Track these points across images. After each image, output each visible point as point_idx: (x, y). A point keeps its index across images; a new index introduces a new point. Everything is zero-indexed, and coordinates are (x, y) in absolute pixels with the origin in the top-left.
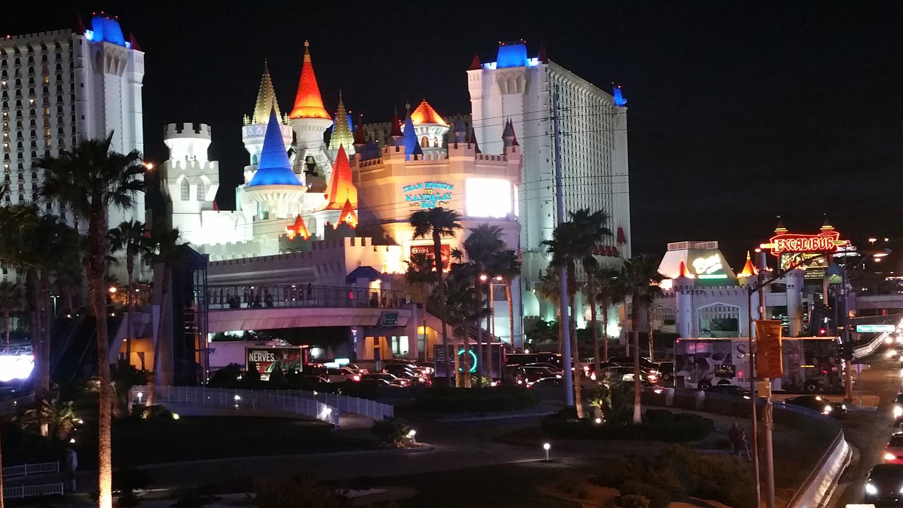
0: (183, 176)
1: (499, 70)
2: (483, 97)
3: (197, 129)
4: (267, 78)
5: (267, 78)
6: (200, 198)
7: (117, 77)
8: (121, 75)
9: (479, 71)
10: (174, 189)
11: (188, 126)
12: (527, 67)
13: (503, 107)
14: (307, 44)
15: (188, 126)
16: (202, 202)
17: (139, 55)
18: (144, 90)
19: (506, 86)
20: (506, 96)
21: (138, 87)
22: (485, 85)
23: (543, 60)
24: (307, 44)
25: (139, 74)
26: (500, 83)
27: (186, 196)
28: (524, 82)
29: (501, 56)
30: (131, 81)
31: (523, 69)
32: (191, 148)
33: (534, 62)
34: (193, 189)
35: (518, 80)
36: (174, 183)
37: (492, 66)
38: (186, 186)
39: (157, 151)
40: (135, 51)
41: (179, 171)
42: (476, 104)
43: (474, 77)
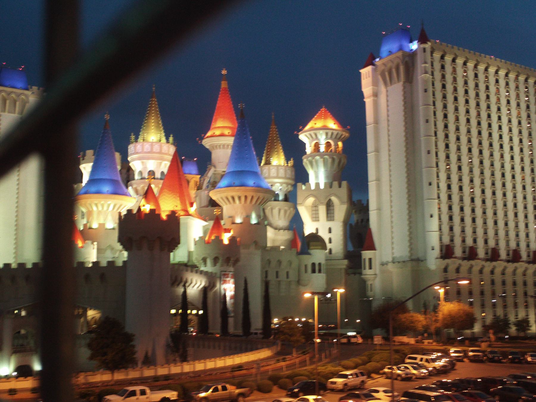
9: (369, 68)
20: (390, 88)
22: (375, 83)
28: (402, 68)
33: (414, 46)
37: (377, 60)
42: (369, 102)
43: (366, 72)
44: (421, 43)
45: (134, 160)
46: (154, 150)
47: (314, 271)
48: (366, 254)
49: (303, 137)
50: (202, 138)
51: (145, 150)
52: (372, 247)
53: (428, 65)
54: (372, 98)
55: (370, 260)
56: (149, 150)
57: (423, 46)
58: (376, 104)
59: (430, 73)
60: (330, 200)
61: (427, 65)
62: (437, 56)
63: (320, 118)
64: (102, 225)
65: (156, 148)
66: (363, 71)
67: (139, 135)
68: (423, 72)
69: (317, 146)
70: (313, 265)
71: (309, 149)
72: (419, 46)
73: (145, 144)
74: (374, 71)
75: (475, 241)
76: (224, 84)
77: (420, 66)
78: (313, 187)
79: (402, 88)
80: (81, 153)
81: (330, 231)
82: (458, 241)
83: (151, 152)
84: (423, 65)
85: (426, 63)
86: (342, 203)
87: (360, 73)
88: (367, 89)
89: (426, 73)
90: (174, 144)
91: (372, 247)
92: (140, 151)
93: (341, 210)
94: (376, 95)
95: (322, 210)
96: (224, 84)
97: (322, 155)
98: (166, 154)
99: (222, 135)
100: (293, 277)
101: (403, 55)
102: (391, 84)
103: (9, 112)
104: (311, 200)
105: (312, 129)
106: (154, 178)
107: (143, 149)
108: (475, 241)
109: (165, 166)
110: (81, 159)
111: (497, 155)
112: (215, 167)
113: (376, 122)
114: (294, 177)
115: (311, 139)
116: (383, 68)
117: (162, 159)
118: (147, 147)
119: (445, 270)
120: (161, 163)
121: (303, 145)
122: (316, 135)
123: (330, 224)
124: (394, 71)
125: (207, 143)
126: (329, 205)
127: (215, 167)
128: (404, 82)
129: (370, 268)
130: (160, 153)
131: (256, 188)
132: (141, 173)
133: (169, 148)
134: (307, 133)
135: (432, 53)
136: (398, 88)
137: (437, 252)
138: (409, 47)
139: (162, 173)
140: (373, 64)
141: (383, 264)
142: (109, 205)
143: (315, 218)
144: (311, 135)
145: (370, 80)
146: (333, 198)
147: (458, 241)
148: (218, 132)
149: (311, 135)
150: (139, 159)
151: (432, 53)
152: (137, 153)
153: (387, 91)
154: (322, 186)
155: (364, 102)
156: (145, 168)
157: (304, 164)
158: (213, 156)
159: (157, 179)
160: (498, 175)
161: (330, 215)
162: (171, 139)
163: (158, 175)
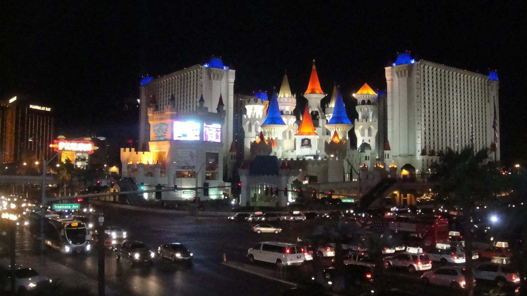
0: (248, 122)
2: (392, 80)
4: (286, 77)
5: (286, 77)
6: (256, 131)
7: (219, 81)
8: (221, 80)
10: (246, 127)
14: (314, 61)
15: (252, 100)
17: (232, 72)
18: (234, 86)
19: (399, 74)
20: (401, 79)
21: (232, 86)
22: (392, 75)
23: (417, 60)
25: (232, 79)
26: (397, 73)
27: (250, 130)
28: (407, 72)
29: (399, 60)
30: (228, 82)
32: (253, 109)
33: (413, 62)
34: (253, 127)
35: (405, 71)
36: (245, 124)
37: (394, 65)
38: (250, 125)
39: (240, 110)
40: (230, 70)
41: (247, 119)
42: (389, 83)
47: (366, 159)
48: (386, 152)
50: (304, 94)
52: (389, 149)
55: (388, 155)
58: (392, 85)
62: (422, 66)
63: (365, 88)
64: (277, 138)
66: (387, 69)
70: (366, 157)
74: (391, 69)
75: (434, 148)
76: (314, 67)
77: (415, 71)
81: (369, 141)
82: (428, 147)
83: (288, 102)
88: (388, 76)
89: (418, 75)
90: (297, 98)
91: (389, 149)
93: (375, 132)
94: (392, 80)
95: (366, 131)
96: (314, 67)
100: (358, 162)
104: (361, 127)
105: (362, 94)
108: (434, 148)
111: (444, 109)
113: (392, 92)
119: (423, 161)
123: (370, 138)
126: (369, 129)
129: (388, 158)
130: (292, 103)
136: (404, 80)
137: (420, 153)
140: (392, 66)
141: (393, 156)
143: (363, 135)
145: (390, 72)
146: (371, 127)
147: (428, 147)
157: (356, 109)
158: (309, 102)
161: (370, 134)
162: (295, 96)
163: (290, 113)
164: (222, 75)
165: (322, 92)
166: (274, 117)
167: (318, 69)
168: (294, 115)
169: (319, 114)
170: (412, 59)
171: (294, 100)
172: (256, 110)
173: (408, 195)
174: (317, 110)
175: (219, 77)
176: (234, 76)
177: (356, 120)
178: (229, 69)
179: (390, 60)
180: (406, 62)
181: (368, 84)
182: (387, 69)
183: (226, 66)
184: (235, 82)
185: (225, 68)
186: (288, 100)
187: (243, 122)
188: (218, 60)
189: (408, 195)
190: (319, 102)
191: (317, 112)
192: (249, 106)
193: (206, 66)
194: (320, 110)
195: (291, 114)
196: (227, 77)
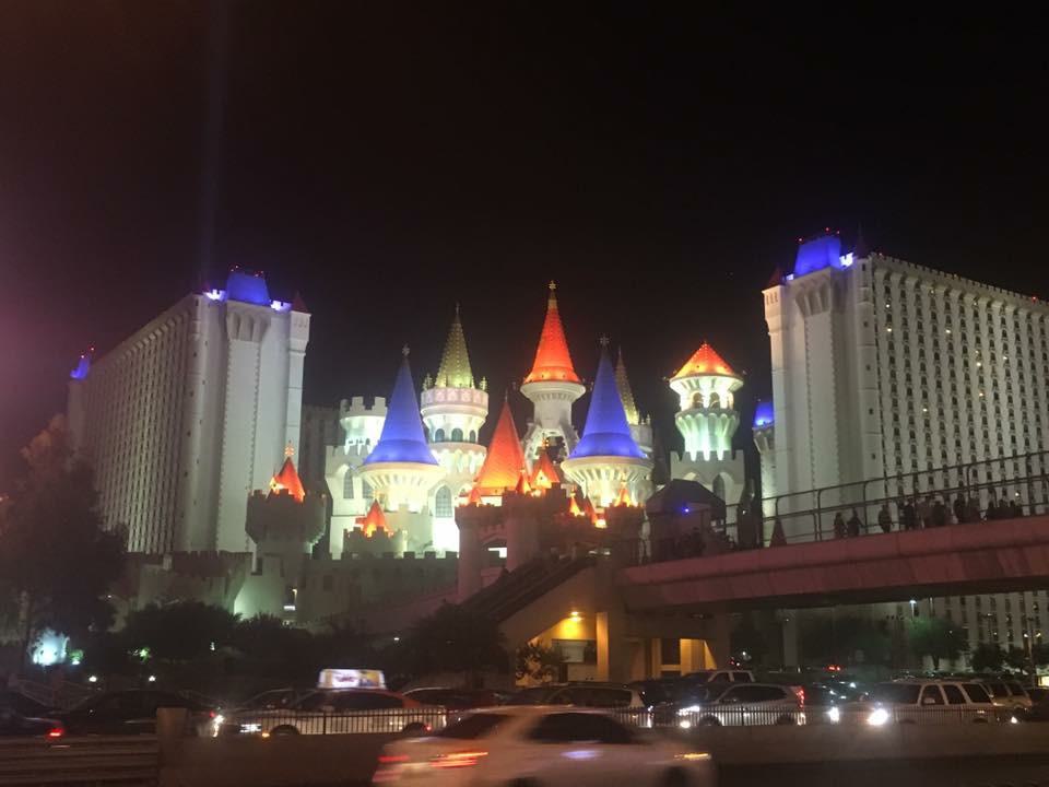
0: (344, 469)
1: (796, 280)
3: (369, 405)
7: (254, 344)
8: (261, 339)
10: (335, 486)
11: (358, 401)
12: (833, 269)
13: (806, 337)
15: (358, 401)
16: (370, 501)
20: (810, 319)
23: (859, 255)
24: (552, 286)
25: (300, 340)
27: (349, 494)
28: (830, 292)
31: (827, 272)
37: (791, 277)
44: (859, 258)
45: (431, 413)
46: (463, 399)
49: (676, 385)
50: (521, 383)
51: (449, 399)
53: (869, 289)
54: (780, 332)
56: (456, 398)
57: (862, 261)
59: (871, 299)
60: (719, 476)
61: (868, 289)
62: (880, 274)
63: (701, 358)
65: (466, 396)
67: (436, 376)
68: (863, 298)
69: (697, 397)
71: (685, 403)
72: (854, 261)
73: (449, 390)
76: (552, 304)
78: (693, 458)
79: (829, 319)
80: (344, 402)
84: (863, 289)
85: (866, 286)
86: (736, 481)
87: (763, 295)
88: (773, 319)
89: (866, 299)
90: (488, 390)
92: (442, 399)
94: (786, 327)
96: (552, 304)
97: (706, 413)
98: (478, 405)
99: (553, 380)
101: (833, 274)
102: (813, 313)
103: (244, 339)
106: (461, 441)
107: (446, 397)
109: (477, 423)
110: (343, 409)
112: (540, 424)
114: (651, 442)
115: (689, 387)
116: (800, 289)
117: (473, 413)
118: (452, 395)
120: (470, 420)
121: (675, 397)
122: (697, 382)
124: (818, 295)
125: (528, 389)
127: (540, 424)
128: (833, 312)
130: (471, 403)
131: (632, 459)
132: (440, 432)
133: (482, 396)
134: (684, 381)
135: (873, 270)
136: (824, 319)
138: (839, 262)
139: (472, 433)
142: (413, 479)
144: (690, 383)
148: (547, 375)
149: (690, 383)
150: (439, 412)
151: (873, 270)
152: (437, 403)
153: (806, 322)
154: (720, 457)
155: (769, 337)
156: (448, 425)
157: (677, 423)
158: (537, 409)
159: (466, 441)
160: (951, 442)
162: (484, 384)
163: (466, 436)
164: (265, 326)
165: (577, 380)
166: (406, 443)
167: (562, 311)
168: (480, 443)
169: (565, 441)
170: (844, 253)
171: (483, 398)
172: (366, 427)
173: (685, 643)
174: (559, 433)
175: (259, 329)
176: (306, 331)
177: (674, 456)
178: (293, 308)
179: (777, 267)
180: (827, 264)
181: (713, 346)
182: (771, 294)
183: (282, 302)
184: (310, 349)
185: (276, 305)
186: (459, 393)
187: (328, 469)
188: (256, 285)
189: (685, 643)
190: (568, 407)
191: (559, 439)
192: (347, 419)
193: (214, 295)
194: (565, 428)
195: (472, 441)
196: (287, 332)
